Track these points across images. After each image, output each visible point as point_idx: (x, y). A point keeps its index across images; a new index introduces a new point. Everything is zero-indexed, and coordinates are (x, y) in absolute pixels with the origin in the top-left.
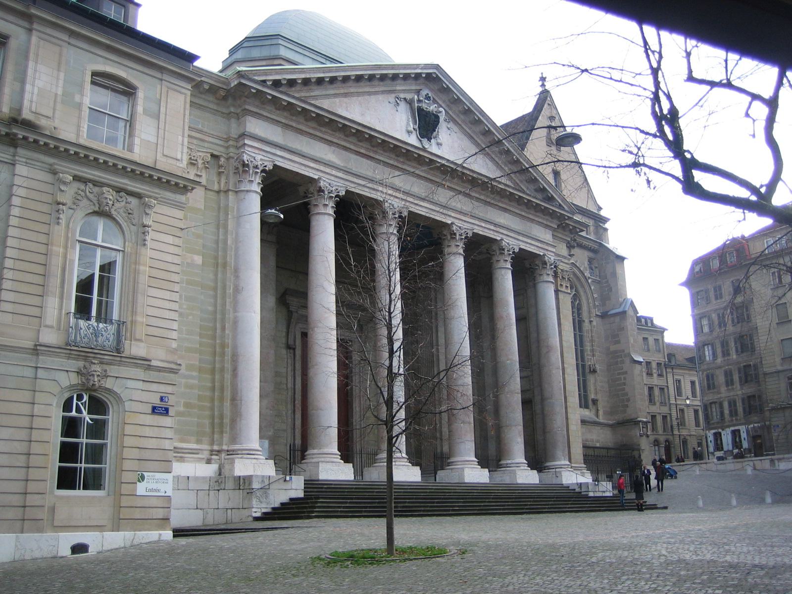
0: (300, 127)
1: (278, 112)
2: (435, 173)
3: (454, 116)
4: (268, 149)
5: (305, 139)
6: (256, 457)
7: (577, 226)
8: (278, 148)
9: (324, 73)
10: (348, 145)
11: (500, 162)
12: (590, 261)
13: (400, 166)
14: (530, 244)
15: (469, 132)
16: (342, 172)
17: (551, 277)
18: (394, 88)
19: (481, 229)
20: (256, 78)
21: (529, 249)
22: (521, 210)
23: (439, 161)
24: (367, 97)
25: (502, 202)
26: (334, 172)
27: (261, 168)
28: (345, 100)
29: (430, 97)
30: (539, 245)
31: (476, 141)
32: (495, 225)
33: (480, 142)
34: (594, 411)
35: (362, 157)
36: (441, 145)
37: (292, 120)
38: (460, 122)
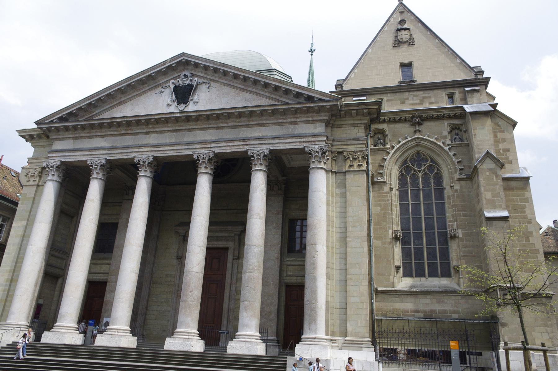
1: (66, 133)
2: (180, 124)
3: (211, 78)
4: (61, 154)
5: (86, 140)
7: (360, 107)
9: (89, 100)
10: (112, 133)
11: (258, 91)
12: (453, 129)
13: (152, 130)
14: (289, 143)
16: (107, 150)
17: (316, 162)
18: (158, 83)
19: (229, 148)
20: (46, 122)
21: (289, 147)
22: (277, 119)
23: (173, 116)
24: (139, 98)
25: (252, 121)
26: (102, 152)
27: (55, 166)
28: (122, 106)
29: (187, 75)
30: (302, 140)
31: (233, 85)
32: (244, 140)
33: (236, 85)
34: (456, 280)
35: (126, 136)
36: (197, 103)
37: (75, 134)
38: (217, 79)
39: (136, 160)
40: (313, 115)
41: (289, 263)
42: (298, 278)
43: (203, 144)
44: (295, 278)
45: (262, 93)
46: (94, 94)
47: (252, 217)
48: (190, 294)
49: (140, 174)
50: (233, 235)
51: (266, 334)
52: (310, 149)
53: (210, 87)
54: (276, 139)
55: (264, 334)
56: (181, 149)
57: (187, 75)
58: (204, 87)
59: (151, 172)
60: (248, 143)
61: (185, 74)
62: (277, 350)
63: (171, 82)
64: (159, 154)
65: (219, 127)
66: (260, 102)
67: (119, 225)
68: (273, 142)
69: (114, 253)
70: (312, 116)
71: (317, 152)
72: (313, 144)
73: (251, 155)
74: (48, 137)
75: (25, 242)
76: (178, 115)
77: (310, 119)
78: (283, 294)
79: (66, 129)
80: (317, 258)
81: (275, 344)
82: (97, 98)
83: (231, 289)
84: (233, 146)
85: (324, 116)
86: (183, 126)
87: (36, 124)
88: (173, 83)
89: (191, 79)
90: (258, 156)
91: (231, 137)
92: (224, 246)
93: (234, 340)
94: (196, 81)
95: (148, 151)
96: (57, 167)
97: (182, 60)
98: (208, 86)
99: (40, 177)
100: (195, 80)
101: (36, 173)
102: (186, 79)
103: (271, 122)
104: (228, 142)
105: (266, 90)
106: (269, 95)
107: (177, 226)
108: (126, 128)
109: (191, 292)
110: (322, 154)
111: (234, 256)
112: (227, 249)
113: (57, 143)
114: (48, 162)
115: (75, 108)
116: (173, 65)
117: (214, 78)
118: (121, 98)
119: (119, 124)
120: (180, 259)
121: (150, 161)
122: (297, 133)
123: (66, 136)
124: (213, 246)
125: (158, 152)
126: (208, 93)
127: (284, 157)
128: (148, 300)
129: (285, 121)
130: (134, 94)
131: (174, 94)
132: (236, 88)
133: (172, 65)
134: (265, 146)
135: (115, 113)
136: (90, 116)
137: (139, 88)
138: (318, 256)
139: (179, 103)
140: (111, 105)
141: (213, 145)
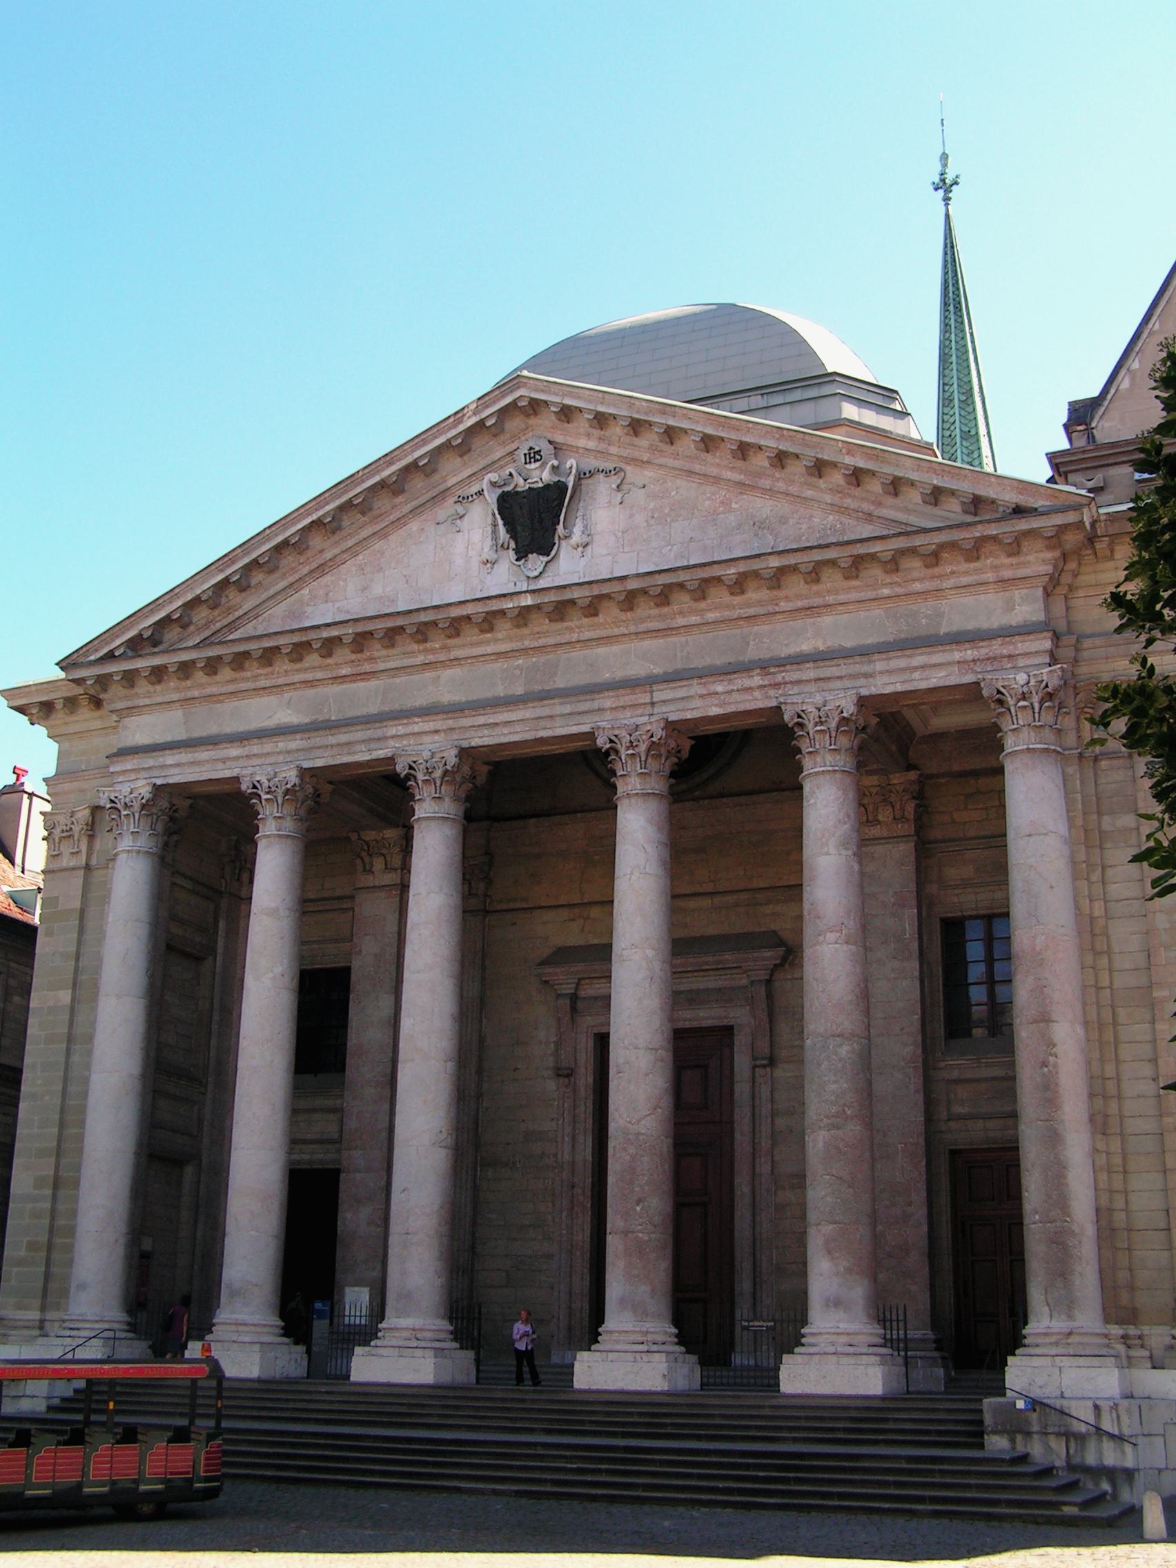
0: (209, 691)
1: (158, 687)
3: (625, 453)
6: (73, 1333)
8: (168, 752)
9: (222, 571)
10: (309, 676)
11: (793, 489)
14: (924, 667)
15: (677, 464)
16: (298, 736)
20: (92, 658)
21: (923, 685)
24: (379, 545)
28: (327, 579)
30: (970, 654)
31: (705, 475)
33: (714, 471)
39: (401, 768)
40: (997, 562)
41: (955, 1074)
42: (991, 1124)
43: (622, 691)
44: (980, 1124)
45: (809, 493)
46: (234, 550)
47: (821, 938)
48: (638, 1208)
49: (419, 813)
50: (744, 981)
51: (901, 1324)
52: (999, 685)
53: (624, 487)
54: (876, 656)
55: (895, 1324)
58: (602, 489)
59: (456, 799)
60: (779, 678)
61: (531, 448)
62: (941, 1372)
63: (486, 480)
64: (479, 739)
66: (804, 526)
67: (353, 978)
68: (865, 668)
69: (347, 1073)
70: (995, 567)
71: (1024, 697)
72: (1010, 665)
73: (796, 720)
74: (97, 703)
75: (75, 1058)
76: (528, 601)
77: (990, 576)
78: (944, 1183)
79: (158, 674)
80: (1055, 1066)
81: (929, 1354)
82: (246, 560)
83: (758, 1170)
84: (733, 691)
85: (1038, 562)
86: (546, 634)
87: (62, 668)
89: (556, 463)
90: (822, 723)
91: (718, 663)
92: (717, 1023)
93: (797, 1350)
94: (574, 471)
95: (436, 732)
96: (143, 807)
97: (514, 403)
98: (614, 481)
99: (91, 837)
100: (571, 468)
101: (76, 829)
102: (538, 464)
103: (854, 596)
104: (711, 679)
105: (821, 483)
106: (836, 500)
107: (545, 963)
108: (354, 657)
109: (638, 1202)
110: (1041, 703)
111: (755, 1059)
112: (726, 1032)
113: (131, 722)
114: (115, 791)
115: (180, 603)
116: (489, 423)
117: (637, 454)
118: (321, 551)
119: (329, 646)
120: (568, 1076)
121: (448, 767)
122: (947, 631)
123: (159, 699)
125: (471, 733)
127: (909, 714)
128: (474, 1223)
129: (900, 590)
130: (365, 533)
131: (500, 522)
132: (717, 480)
133: (481, 424)
134: (839, 684)
136: (225, 622)
137: (378, 512)
138: (1059, 1061)
139: (521, 554)
140: (292, 579)
141: (658, 696)
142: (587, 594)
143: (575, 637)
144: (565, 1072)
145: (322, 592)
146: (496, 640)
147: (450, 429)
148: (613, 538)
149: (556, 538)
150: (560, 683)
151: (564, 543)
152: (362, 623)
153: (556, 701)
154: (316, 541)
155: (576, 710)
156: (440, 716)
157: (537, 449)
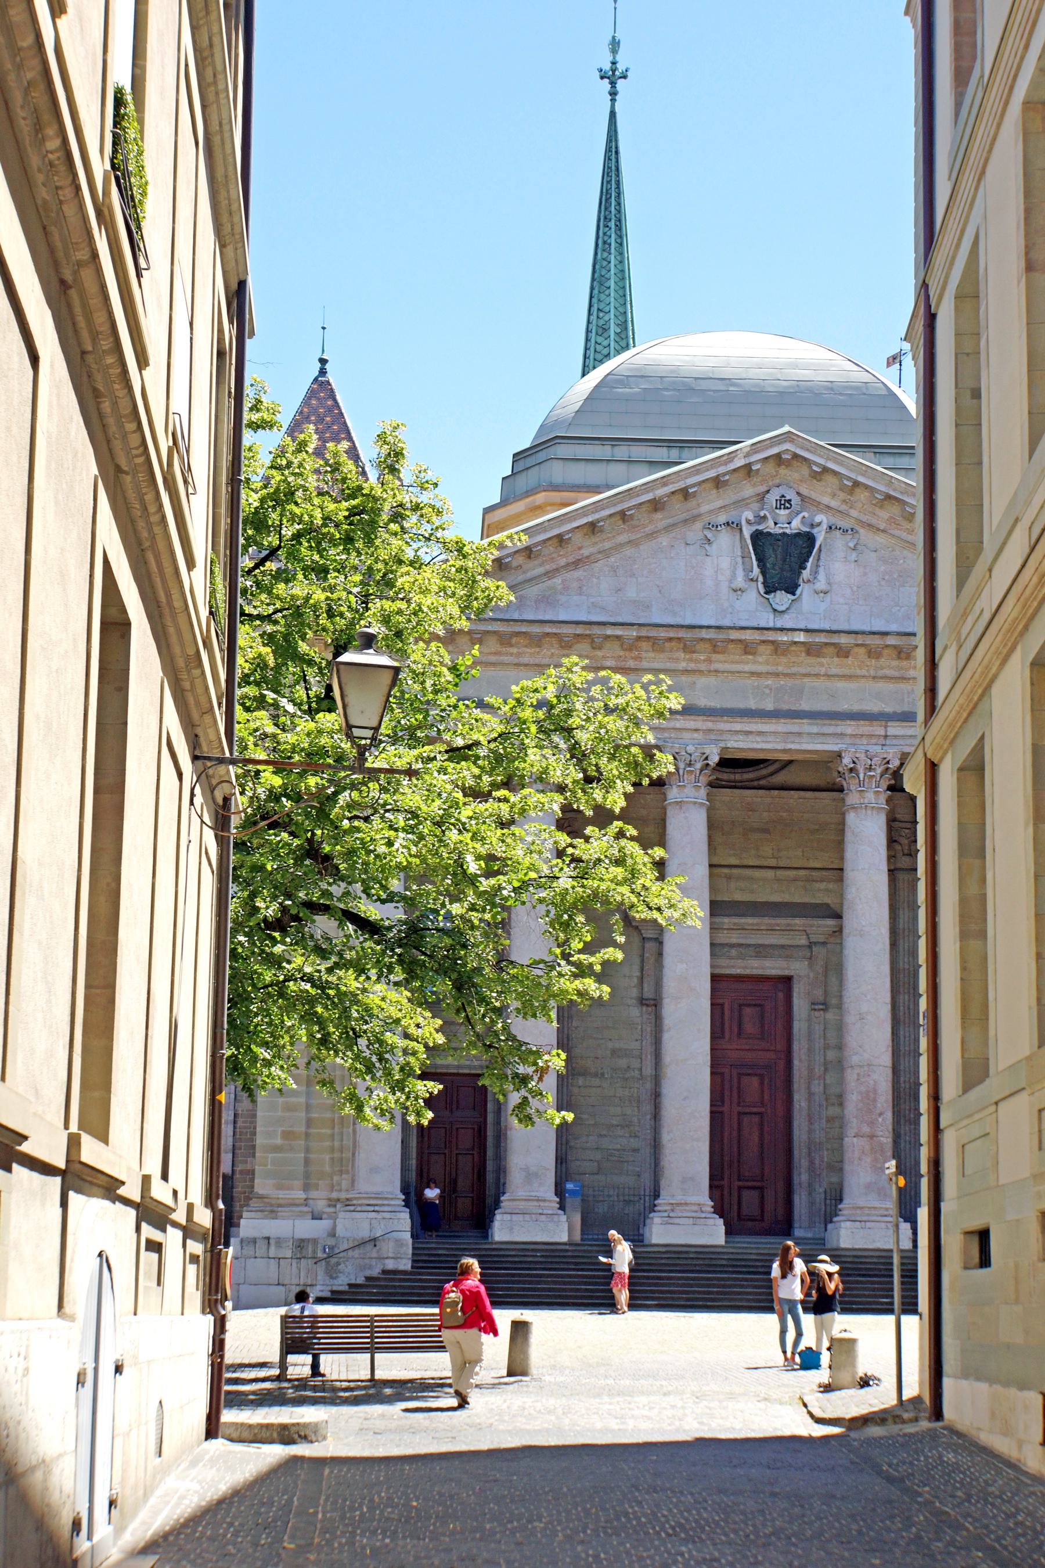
2: (793, 659)
3: (864, 518)
13: (703, 667)
18: (695, 512)
23: (785, 639)
24: (629, 551)
29: (789, 501)
56: (799, 734)
57: (789, 501)
61: (783, 496)
65: (905, 679)
88: (748, 522)
89: (806, 514)
95: (696, 730)
102: (787, 511)
108: (622, 653)
116: (754, 468)
117: (874, 521)
118: (580, 548)
124: (748, 972)
126: (853, 565)
130: (623, 538)
131: (754, 557)
133: (748, 467)
135: (561, 593)
139: (770, 589)
140: (548, 567)
142: (853, 641)
143: (823, 671)
144: (652, 1002)
145: (575, 585)
146: (755, 662)
147: (721, 465)
148: (848, 591)
149: (801, 580)
150: (805, 706)
151: (806, 586)
152: (646, 628)
153: (805, 721)
154: (578, 538)
155: (822, 732)
156: (701, 718)
157: (788, 498)
